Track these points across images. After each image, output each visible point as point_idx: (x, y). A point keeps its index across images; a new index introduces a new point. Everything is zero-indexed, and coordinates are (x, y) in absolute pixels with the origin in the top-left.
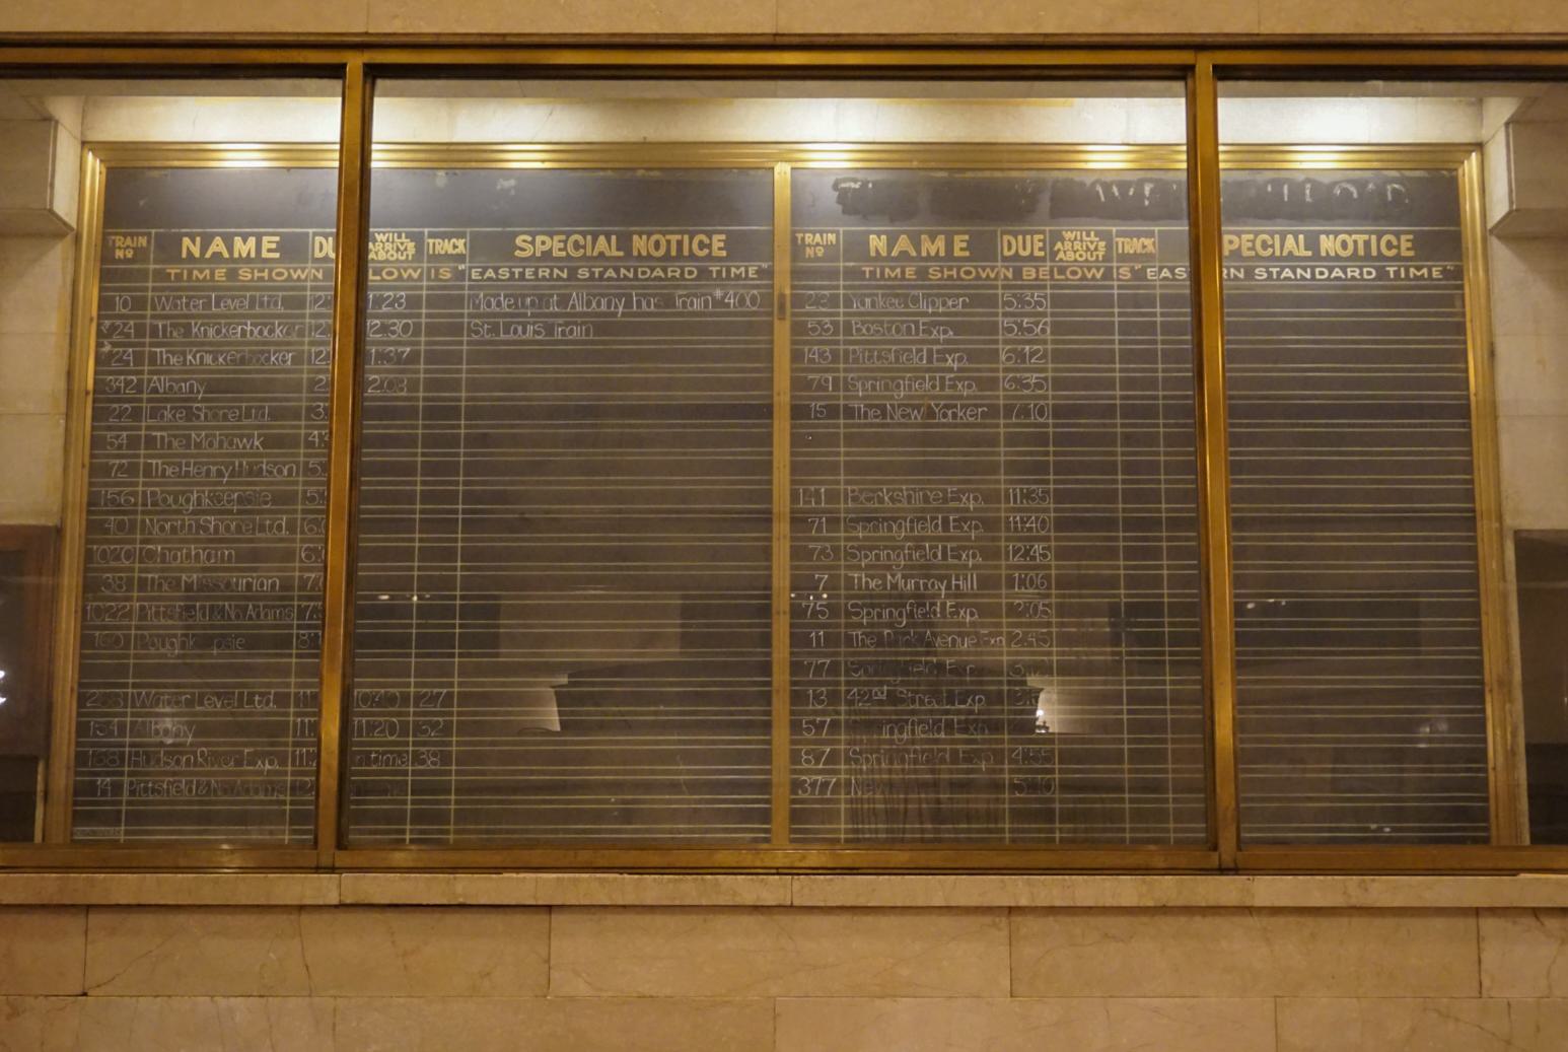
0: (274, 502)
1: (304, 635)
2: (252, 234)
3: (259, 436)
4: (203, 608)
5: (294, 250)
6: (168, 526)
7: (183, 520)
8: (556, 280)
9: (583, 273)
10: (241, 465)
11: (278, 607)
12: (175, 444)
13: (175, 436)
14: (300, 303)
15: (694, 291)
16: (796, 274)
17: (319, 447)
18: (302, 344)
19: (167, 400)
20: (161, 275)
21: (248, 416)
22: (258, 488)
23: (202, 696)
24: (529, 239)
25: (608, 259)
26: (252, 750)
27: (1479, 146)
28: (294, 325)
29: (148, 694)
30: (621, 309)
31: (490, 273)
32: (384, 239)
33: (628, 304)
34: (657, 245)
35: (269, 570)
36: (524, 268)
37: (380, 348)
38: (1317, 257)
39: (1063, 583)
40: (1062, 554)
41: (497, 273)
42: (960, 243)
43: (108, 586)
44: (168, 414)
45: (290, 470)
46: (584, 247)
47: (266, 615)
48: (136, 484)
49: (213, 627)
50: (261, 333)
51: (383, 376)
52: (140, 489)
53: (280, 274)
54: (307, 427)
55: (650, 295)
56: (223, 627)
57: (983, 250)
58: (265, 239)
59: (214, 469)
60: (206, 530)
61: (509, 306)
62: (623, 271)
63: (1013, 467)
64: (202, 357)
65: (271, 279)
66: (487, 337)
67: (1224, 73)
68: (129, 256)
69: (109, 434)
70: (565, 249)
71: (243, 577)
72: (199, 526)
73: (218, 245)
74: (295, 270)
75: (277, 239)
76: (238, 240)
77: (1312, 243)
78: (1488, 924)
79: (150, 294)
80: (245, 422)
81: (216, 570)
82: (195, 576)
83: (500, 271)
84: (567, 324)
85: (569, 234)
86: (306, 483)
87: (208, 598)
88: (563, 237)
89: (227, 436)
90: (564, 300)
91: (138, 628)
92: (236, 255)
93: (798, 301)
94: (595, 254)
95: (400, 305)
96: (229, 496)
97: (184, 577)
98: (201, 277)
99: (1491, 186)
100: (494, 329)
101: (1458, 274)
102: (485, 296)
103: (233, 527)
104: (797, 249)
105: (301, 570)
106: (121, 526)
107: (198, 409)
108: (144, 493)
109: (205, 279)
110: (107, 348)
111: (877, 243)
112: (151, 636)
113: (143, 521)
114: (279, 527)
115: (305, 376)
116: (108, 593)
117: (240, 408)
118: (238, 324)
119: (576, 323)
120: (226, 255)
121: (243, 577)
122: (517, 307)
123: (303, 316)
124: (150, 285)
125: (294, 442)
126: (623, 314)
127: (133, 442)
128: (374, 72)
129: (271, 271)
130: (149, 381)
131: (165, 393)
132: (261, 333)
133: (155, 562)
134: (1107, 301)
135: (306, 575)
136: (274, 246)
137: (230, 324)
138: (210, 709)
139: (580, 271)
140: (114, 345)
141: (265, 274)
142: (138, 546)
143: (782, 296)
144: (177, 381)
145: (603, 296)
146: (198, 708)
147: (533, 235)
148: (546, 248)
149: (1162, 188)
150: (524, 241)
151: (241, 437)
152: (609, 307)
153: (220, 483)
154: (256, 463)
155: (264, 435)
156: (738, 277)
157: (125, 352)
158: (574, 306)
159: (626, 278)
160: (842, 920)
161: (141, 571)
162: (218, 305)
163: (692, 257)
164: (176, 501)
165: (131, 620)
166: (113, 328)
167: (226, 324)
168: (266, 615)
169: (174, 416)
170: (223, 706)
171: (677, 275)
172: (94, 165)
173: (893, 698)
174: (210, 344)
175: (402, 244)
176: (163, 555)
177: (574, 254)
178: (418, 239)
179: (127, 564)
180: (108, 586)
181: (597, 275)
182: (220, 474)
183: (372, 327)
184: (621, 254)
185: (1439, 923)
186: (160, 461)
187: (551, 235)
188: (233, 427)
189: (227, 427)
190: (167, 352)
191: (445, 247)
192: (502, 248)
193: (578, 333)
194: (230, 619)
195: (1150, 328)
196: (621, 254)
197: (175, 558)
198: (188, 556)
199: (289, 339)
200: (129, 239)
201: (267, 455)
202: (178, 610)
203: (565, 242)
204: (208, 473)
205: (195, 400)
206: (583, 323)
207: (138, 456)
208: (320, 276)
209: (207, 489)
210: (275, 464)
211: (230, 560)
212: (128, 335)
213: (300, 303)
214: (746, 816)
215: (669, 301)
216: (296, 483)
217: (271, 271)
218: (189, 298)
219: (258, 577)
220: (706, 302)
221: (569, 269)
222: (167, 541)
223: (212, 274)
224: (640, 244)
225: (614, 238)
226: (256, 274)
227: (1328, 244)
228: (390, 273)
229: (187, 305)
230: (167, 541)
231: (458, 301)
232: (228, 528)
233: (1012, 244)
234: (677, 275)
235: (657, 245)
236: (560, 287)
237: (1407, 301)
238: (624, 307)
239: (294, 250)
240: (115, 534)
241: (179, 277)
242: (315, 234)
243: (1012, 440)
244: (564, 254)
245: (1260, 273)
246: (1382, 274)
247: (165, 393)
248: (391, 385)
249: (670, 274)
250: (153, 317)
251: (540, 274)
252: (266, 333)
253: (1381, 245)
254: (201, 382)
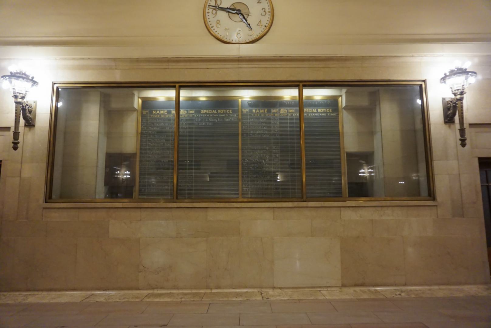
5: (169, 112)
16: (242, 115)
20: (150, 116)
27: (341, 96)
38: (318, 112)
39: (281, 160)
40: (281, 156)
42: (266, 111)
57: (269, 112)
63: (274, 143)
67: (305, 86)
73: (158, 112)
77: (317, 110)
78: (342, 209)
90: (208, 119)
93: (242, 119)
99: (343, 102)
101: (338, 114)
104: (242, 112)
111: (254, 111)
127: (146, 141)
128: (180, 87)
134: (287, 119)
149: (295, 102)
160: (249, 209)
172: (140, 100)
173: (256, 177)
178: (187, 111)
185: (335, 209)
191: (191, 112)
192: (199, 112)
193: (210, 124)
195: (293, 123)
213: (170, 120)
214: (235, 194)
215: (223, 119)
224: (219, 111)
227: (319, 110)
231: (193, 120)
233: (273, 111)
237: (332, 118)
239: (169, 112)
243: (274, 139)
245: (309, 115)
246: (327, 115)
253: (327, 110)
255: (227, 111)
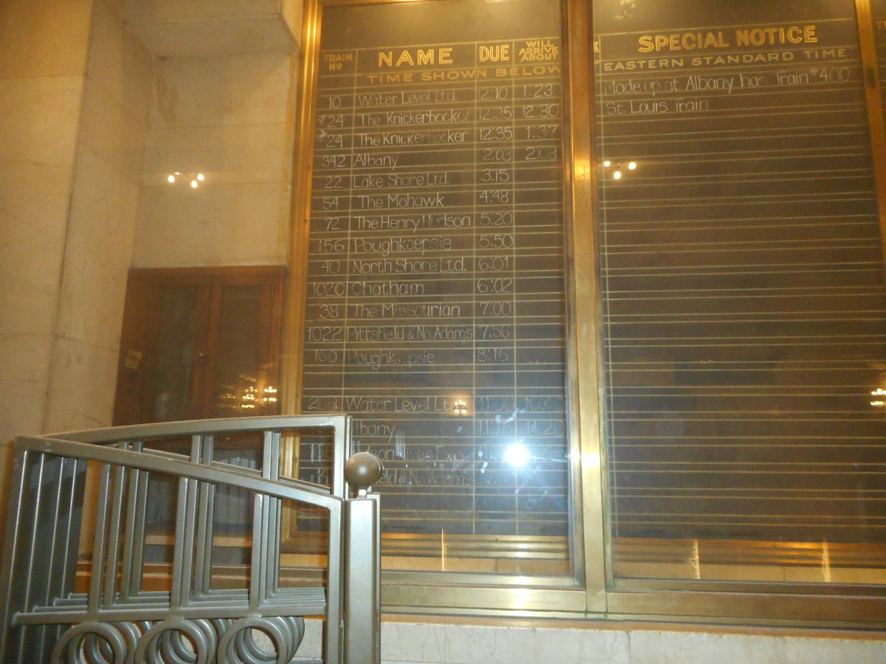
0: (454, 246)
1: (482, 351)
2: (431, 48)
3: (440, 196)
4: (400, 329)
6: (371, 266)
7: (383, 262)
8: (674, 68)
9: (697, 61)
10: (427, 218)
11: (460, 329)
12: (375, 203)
13: (375, 198)
14: (470, 95)
15: (791, 70)
17: (489, 203)
18: (472, 125)
19: (368, 171)
20: (363, 81)
21: (432, 180)
22: (441, 236)
23: (400, 402)
24: (650, 38)
25: (718, 49)
26: (442, 445)
28: (465, 112)
29: (357, 399)
30: (731, 87)
31: (620, 66)
32: (534, 45)
33: (737, 83)
34: (757, 37)
35: (450, 299)
36: (648, 60)
37: (534, 126)
41: (625, 65)
43: (325, 314)
44: (369, 182)
45: (466, 221)
46: (696, 42)
47: (450, 336)
48: (346, 235)
49: (408, 345)
50: (440, 118)
51: (538, 147)
52: (349, 238)
53: (453, 75)
54: (478, 188)
55: (754, 75)
56: (415, 345)
58: (441, 51)
59: (406, 222)
60: (401, 268)
61: (637, 90)
62: (729, 58)
64: (395, 139)
65: (446, 79)
66: (621, 114)
68: (339, 68)
69: (325, 198)
70: (680, 44)
71: (430, 305)
72: (395, 266)
73: (405, 57)
74: (465, 72)
75: (451, 50)
76: (420, 53)
79: (355, 94)
80: (430, 185)
81: (409, 299)
82: (392, 305)
83: (628, 64)
84: (685, 101)
85: (682, 33)
86: (478, 231)
87: (402, 322)
88: (678, 36)
89: (415, 196)
90: (682, 83)
91: (348, 346)
92: (419, 63)
94: (706, 46)
95: (549, 93)
96: (418, 242)
97: (384, 306)
98: (393, 80)
100: (626, 107)
102: (617, 83)
103: (422, 265)
105: (477, 298)
106: (334, 267)
107: (392, 177)
108: (352, 241)
109: (396, 82)
110: (323, 135)
112: (359, 352)
113: (352, 263)
114: (459, 266)
115: (475, 149)
116: (324, 319)
117: (425, 176)
118: (422, 113)
119: (694, 101)
120: (412, 63)
121: (430, 305)
122: (643, 90)
123: (473, 105)
124: (355, 88)
125: (468, 199)
126: (733, 92)
127: (343, 204)
129: (446, 73)
130: (355, 157)
131: (367, 166)
132: (440, 118)
133: (361, 294)
135: (482, 302)
136: (448, 55)
137: (416, 113)
138: (407, 412)
139: (694, 60)
140: (328, 132)
141: (442, 76)
142: (348, 282)
143: (870, 70)
144: (377, 157)
145: (716, 78)
146: (397, 411)
147: (653, 35)
148: (664, 44)
150: (647, 40)
151: (426, 197)
152: (720, 86)
153: (411, 233)
154: (439, 217)
155: (445, 195)
156: (829, 57)
157: (336, 138)
158: (690, 87)
159: (733, 63)
161: (350, 301)
162: (406, 100)
163: (788, 44)
164: (376, 247)
165: (342, 340)
166: (327, 121)
167: (412, 114)
168: (450, 336)
169: (374, 183)
170: (417, 409)
171: (776, 58)
174: (401, 128)
175: (548, 48)
176: (367, 289)
177: (687, 47)
179: (339, 296)
180: (325, 314)
181: (708, 63)
182: (411, 225)
183: (526, 111)
184: (727, 45)
186: (364, 217)
187: (668, 35)
188: (421, 190)
189: (416, 190)
190: (368, 136)
193: (696, 107)
194: (421, 338)
196: (727, 45)
197: (377, 291)
198: (387, 288)
199: (462, 122)
200: (339, 56)
201: (448, 210)
202: (380, 332)
203: (680, 39)
204: (401, 224)
205: (390, 171)
206: (698, 100)
207: (347, 214)
208: (484, 75)
209: (401, 237)
210: (454, 217)
211: (420, 292)
212: (339, 125)
213: (470, 95)
215: (771, 79)
216: (471, 231)
217: (446, 73)
218: (384, 96)
219: (443, 305)
220: (804, 79)
221: (685, 59)
222: (369, 278)
223: (402, 77)
224: (743, 37)
225: (720, 34)
226: (435, 76)
228: (539, 70)
229: (383, 101)
230: (369, 278)
232: (417, 267)
234: (776, 58)
235: (757, 37)
236: (678, 73)
238: (734, 85)
240: (329, 273)
241: (376, 81)
242: (479, 45)
244: (679, 48)
247: (367, 166)
248: (544, 153)
249: (770, 58)
250: (357, 111)
251: (661, 65)
252: (443, 119)
254: (394, 157)
255: (788, 35)
